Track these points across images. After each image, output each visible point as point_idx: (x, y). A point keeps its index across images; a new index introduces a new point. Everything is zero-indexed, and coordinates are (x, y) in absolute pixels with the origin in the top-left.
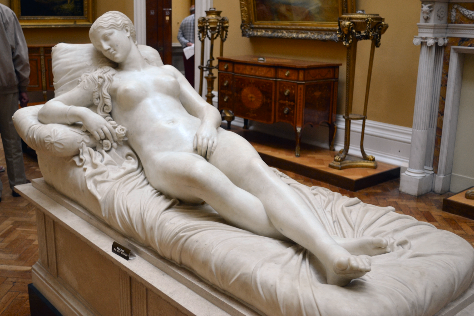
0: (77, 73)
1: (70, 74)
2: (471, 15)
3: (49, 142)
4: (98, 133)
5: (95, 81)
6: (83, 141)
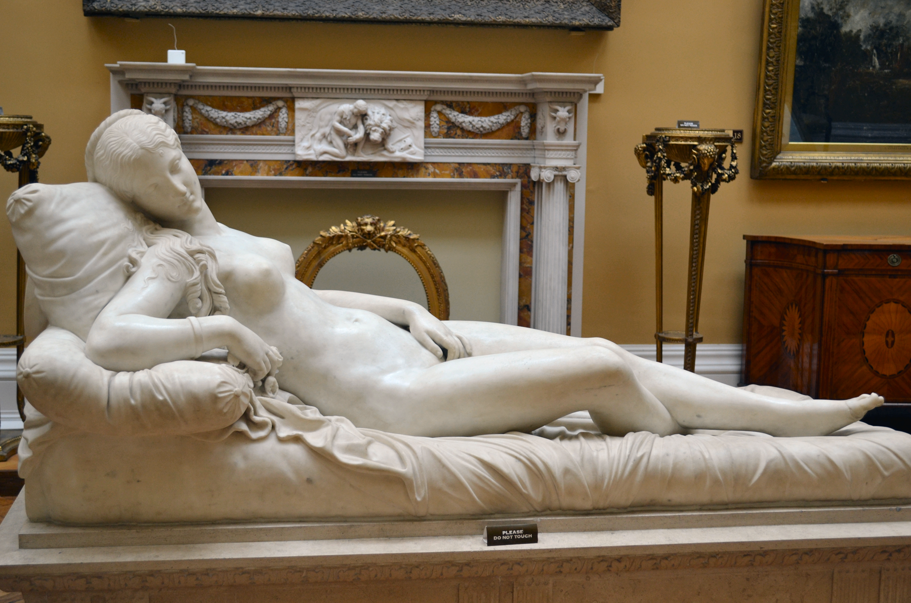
0: (119, 249)
1: (105, 254)
2: (223, 118)
3: (229, 395)
5: (186, 262)
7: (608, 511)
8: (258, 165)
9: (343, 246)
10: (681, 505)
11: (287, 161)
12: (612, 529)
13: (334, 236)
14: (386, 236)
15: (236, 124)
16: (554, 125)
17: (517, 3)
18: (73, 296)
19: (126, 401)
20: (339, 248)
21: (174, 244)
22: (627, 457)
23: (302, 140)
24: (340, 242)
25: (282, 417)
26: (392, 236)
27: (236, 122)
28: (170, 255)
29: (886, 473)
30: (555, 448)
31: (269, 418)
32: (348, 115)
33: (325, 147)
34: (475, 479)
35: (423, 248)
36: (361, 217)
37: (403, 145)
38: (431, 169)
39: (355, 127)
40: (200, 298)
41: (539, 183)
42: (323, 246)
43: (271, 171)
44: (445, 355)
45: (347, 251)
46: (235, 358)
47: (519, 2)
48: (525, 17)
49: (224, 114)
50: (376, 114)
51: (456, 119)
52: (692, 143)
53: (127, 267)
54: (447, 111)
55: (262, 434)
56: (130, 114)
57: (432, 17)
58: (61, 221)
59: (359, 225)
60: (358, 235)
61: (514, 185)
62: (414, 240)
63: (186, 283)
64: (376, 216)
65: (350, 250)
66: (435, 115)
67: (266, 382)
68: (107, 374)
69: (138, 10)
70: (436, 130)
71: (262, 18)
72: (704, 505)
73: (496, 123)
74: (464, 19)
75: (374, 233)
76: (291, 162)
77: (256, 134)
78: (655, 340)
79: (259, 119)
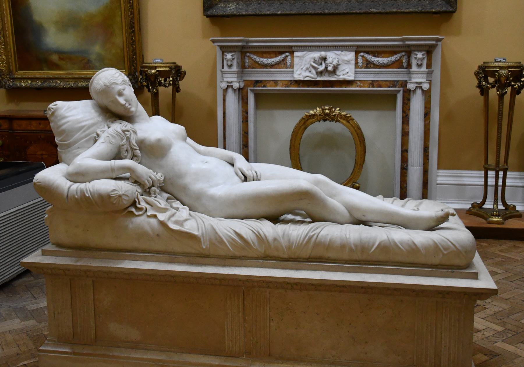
0: (91, 130)
1: (84, 131)
2: (262, 61)
3: (116, 196)
4: (148, 181)
5: (120, 135)
6: (137, 191)
7: (298, 260)
8: (278, 83)
9: (315, 120)
10: (335, 260)
11: (291, 81)
12: (297, 269)
13: (311, 115)
14: (335, 115)
15: (267, 64)
16: (416, 62)
17: (404, 2)
18: (69, 149)
19: (74, 196)
20: (313, 121)
21: (117, 128)
22: (305, 234)
23: (297, 71)
24: (314, 117)
25: (152, 206)
26: (338, 115)
27: (267, 63)
28: (114, 132)
29: (445, 252)
30: (272, 228)
31: (145, 206)
32: (317, 59)
33: (307, 74)
34: (231, 240)
35: (353, 121)
36: (324, 106)
37: (344, 72)
38: (359, 83)
39: (321, 64)
40: (127, 151)
41: (410, 90)
42: (306, 119)
43: (283, 85)
44: (246, 179)
45: (318, 122)
46: (133, 178)
47: (405, 1)
48: (407, 9)
49: (262, 59)
50: (330, 58)
51: (370, 60)
52: (496, 69)
53: (95, 137)
54: (366, 55)
55: (141, 213)
56: (108, 70)
57: (360, 11)
58: (65, 117)
59: (323, 110)
60: (322, 114)
61: (399, 91)
62: (348, 117)
63: (120, 145)
64: (331, 105)
65: (319, 121)
66: (360, 58)
67: (151, 190)
68: (69, 183)
69: (226, 14)
70: (361, 65)
71: (281, 15)
72: (347, 261)
73: (390, 61)
74: (376, 11)
75: (329, 113)
76: (293, 81)
77: (276, 68)
78: (483, 168)
79: (278, 61)
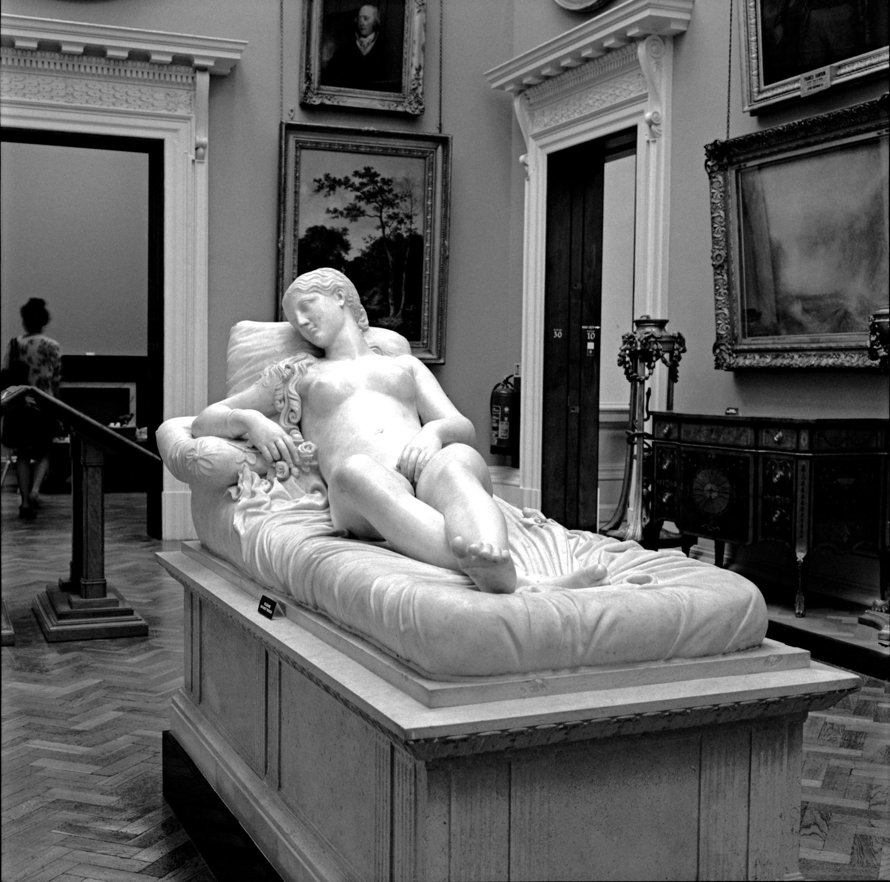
0: (260, 364)
1: (249, 366)
4: (269, 449)
6: (245, 461)
